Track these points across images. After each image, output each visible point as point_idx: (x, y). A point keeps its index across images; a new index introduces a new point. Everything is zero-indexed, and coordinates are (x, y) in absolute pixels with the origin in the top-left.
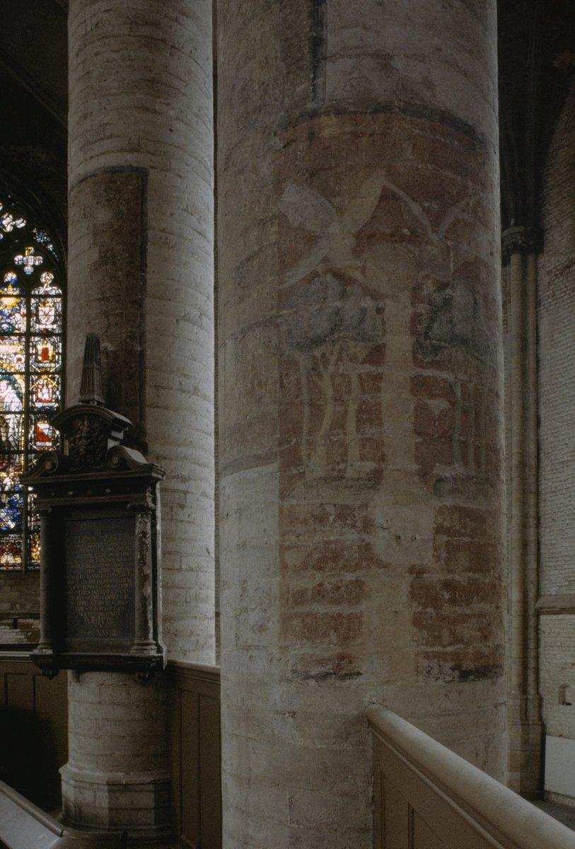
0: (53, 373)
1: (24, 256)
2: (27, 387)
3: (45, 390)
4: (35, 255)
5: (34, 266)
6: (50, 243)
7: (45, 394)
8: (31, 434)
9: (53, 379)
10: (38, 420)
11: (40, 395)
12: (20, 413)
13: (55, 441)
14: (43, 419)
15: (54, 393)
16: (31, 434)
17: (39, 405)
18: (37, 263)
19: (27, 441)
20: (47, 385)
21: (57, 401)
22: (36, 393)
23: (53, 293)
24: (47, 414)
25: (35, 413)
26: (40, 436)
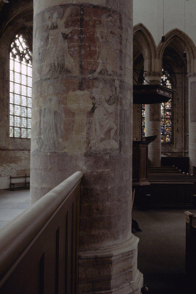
0: (169, 102)
4: (165, 77)
5: (165, 79)
6: (168, 74)
8: (165, 115)
9: (170, 103)
10: (166, 112)
11: (167, 106)
12: (163, 110)
13: (170, 116)
15: (170, 106)
16: (165, 115)
17: (167, 108)
18: (166, 78)
19: (164, 116)
20: (168, 104)
21: (170, 108)
22: (166, 106)
23: (169, 85)
24: (168, 110)
25: (166, 110)
26: (167, 115)
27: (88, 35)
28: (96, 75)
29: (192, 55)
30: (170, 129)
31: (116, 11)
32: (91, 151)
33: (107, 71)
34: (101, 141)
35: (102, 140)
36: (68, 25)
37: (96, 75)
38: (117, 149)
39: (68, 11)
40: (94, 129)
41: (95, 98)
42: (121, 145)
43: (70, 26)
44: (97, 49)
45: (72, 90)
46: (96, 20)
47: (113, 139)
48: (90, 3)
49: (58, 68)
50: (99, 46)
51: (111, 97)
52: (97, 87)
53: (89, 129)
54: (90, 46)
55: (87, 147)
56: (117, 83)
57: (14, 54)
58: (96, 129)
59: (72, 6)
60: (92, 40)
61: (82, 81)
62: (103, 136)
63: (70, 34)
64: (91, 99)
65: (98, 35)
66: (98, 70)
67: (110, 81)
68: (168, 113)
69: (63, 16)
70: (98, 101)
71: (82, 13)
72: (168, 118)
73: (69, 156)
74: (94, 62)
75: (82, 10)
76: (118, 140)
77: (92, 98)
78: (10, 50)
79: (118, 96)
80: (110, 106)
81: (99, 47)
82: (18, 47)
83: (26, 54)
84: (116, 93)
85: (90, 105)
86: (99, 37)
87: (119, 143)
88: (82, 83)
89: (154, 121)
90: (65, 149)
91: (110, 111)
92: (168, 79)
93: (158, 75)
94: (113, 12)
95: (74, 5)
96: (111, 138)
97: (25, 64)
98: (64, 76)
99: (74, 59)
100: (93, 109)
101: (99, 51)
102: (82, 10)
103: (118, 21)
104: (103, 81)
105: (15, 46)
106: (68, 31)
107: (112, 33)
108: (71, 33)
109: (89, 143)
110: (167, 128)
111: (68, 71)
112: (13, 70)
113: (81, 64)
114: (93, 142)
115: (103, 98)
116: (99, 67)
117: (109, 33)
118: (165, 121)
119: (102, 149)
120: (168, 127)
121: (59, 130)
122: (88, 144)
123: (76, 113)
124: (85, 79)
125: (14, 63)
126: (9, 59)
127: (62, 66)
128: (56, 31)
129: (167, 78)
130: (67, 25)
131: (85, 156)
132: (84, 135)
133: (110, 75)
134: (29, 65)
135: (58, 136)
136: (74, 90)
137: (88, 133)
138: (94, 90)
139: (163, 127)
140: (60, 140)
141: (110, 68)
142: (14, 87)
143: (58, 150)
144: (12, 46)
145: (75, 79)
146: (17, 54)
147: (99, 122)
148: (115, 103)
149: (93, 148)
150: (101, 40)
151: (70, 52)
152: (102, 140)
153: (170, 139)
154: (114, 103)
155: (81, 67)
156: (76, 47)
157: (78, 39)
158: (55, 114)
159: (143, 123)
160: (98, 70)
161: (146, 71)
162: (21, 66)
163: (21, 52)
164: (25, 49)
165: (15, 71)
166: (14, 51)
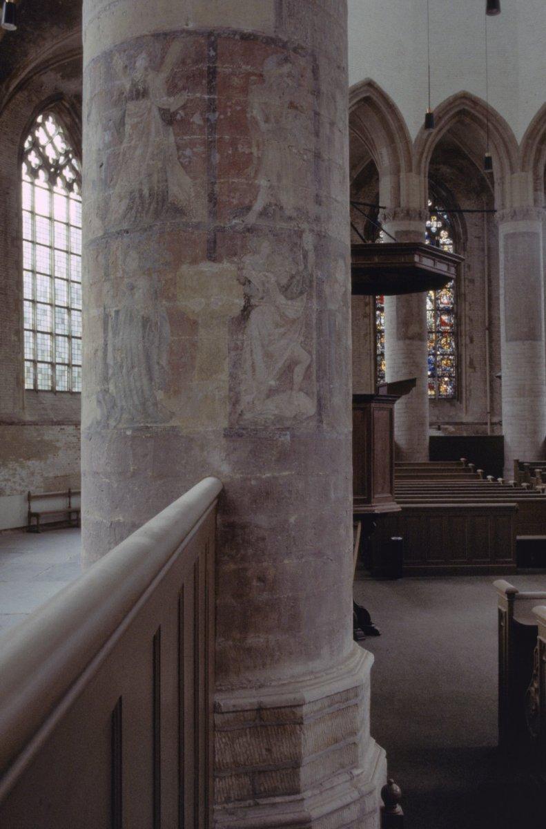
1: (431, 221)
2: (435, 296)
3: (445, 298)
4: (437, 221)
5: (437, 228)
7: (445, 300)
8: (438, 323)
9: (449, 291)
10: (441, 314)
11: (442, 300)
12: (432, 310)
13: (451, 326)
14: (444, 314)
15: (450, 299)
17: (442, 306)
18: (438, 226)
19: (436, 326)
20: (446, 295)
21: (452, 304)
22: (440, 299)
23: (448, 243)
24: (447, 311)
25: (440, 311)
26: (443, 323)
27: (229, 114)
28: (251, 218)
29: (506, 162)
30: (450, 360)
31: (302, 48)
32: (241, 423)
33: (281, 208)
34: (268, 396)
35: (271, 393)
36: (176, 86)
37: (251, 218)
38: (311, 417)
39: (176, 49)
40: (249, 363)
41: (249, 281)
42: (320, 406)
43: (180, 90)
44: (254, 150)
45: (188, 261)
46: (249, 74)
47: (301, 390)
48: (234, 26)
49: (150, 204)
50: (258, 141)
51: (292, 277)
52: (255, 252)
53: (236, 364)
54: (233, 143)
55: (230, 414)
56: (309, 241)
57: (34, 166)
58: (253, 363)
59: (184, 35)
60: (240, 125)
61: (215, 235)
62: (273, 383)
63: (180, 112)
64: (240, 283)
65: (255, 112)
66: (258, 206)
67: (289, 236)
68: (445, 318)
69: (162, 63)
70: (258, 289)
71: (212, 53)
72: (447, 332)
73: (182, 437)
74: (247, 184)
75: (213, 45)
76: (313, 393)
77: (242, 281)
78: (22, 156)
79: (311, 275)
80: (290, 302)
81: (258, 146)
82: (44, 147)
83: (63, 167)
84: (306, 267)
85: (237, 301)
86: (259, 118)
87: (316, 401)
88: (215, 242)
89: (408, 342)
90: (173, 419)
91: (291, 314)
92: (444, 227)
93: (417, 218)
94: (295, 50)
95: (189, 33)
96: (296, 387)
97: (64, 192)
98: (168, 224)
99: (194, 178)
100: (247, 310)
101: (260, 155)
102: (213, 48)
103: (309, 74)
104: (271, 236)
105: (35, 144)
106: (174, 103)
107: (292, 105)
108: (184, 107)
109: (235, 402)
110: (442, 359)
111: (178, 211)
112: (29, 209)
113: (213, 190)
114: (246, 399)
115: (273, 279)
116: (259, 198)
117: (286, 106)
118: (437, 341)
119: (273, 418)
120: (446, 354)
121: (157, 367)
122: (234, 405)
123: (200, 322)
124: (222, 230)
125: (33, 191)
126: (20, 180)
127: (160, 198)
128: (143, 103)
129: (443, 224)
130: (172, 89)
131: (225, 436)
132: (224, 381)
133: (290, 218)
134: (72, 195)
135: (153, 383)
136: (194, 261)
137: (233, 376)
138: (248, 259)
139: (432, 357)
140: (160, 395)
141: (288, 201)
142: (34, 255)
143: (156, 422)
144: (27, 145)
145: (196, 232)
146: (40, 167)
147: (263, 346)
148: (305, 295)
149: (248, 416)
150: (263, 126)
151: (181, 160)
152: (271, 393)
153: (451, 389)
154: (302, 293)
155: (212, 199)
156: (197, 146)
157: (201, 123)
158: (144, 326)
159: (379, 345)
160: (258, 206)
161: (384, 208)
162: (51, 197)
163: (51, 161)
164: (61, 154)
165: (37, 211)
166: (33, 159)
